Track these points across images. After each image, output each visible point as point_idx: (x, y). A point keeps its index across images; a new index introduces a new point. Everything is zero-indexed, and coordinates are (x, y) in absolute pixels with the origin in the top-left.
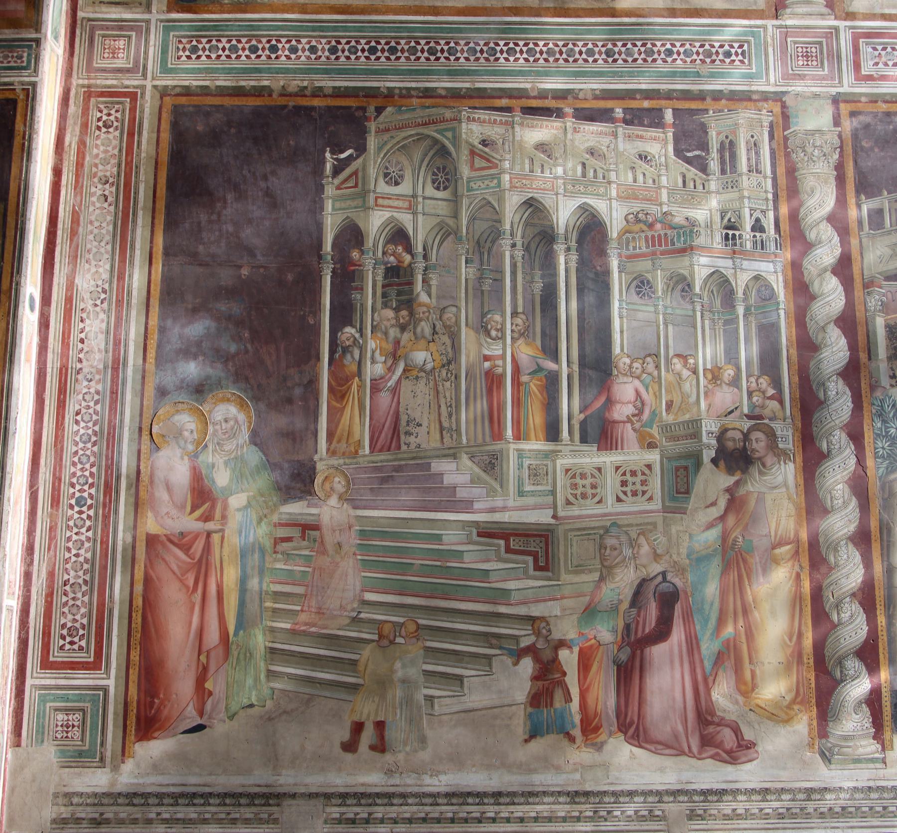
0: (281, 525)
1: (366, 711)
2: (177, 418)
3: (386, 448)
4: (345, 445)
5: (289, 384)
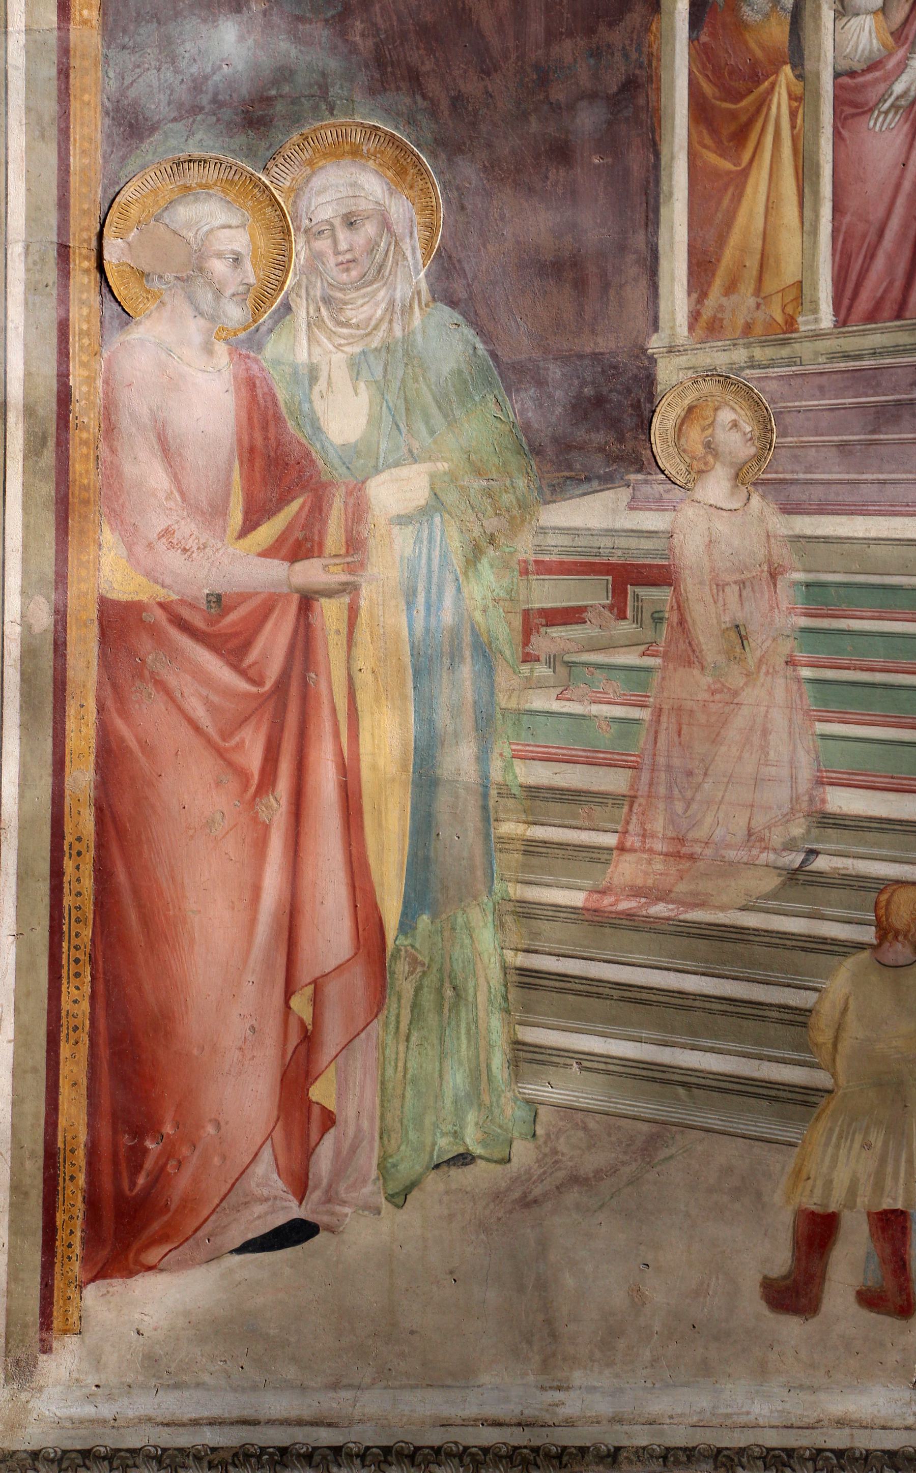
0: (543, 568)
1: (842, 1177)
2: (184, 213)
3: (889, 308)
4: (751, 301)
5: (559, 94)
